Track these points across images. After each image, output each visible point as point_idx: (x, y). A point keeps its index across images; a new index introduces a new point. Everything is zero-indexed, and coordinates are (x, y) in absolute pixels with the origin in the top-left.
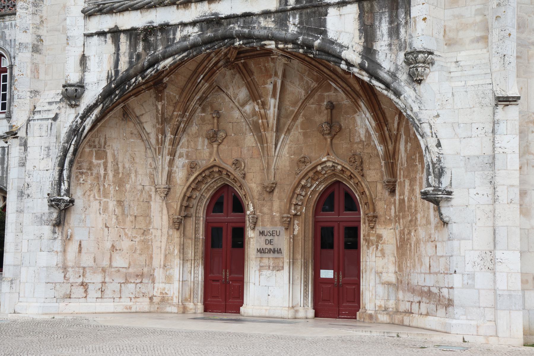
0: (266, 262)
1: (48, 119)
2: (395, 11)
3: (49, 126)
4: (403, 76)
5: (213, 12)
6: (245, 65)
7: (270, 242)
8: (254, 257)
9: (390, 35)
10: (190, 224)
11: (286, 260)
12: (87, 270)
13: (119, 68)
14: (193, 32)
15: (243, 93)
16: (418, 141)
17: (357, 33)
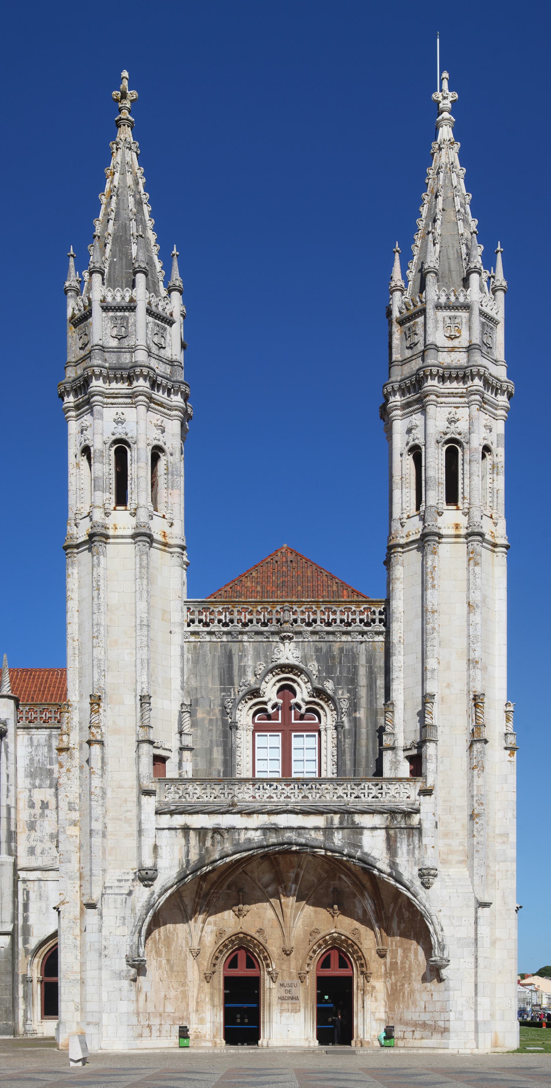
0: (285, 1006)
1: (122, 894)
2: (411, 840)
3: (124, 900)
4: (418, 882)
5: (273, 822)
7: (289, 991)
8: (276, 1003)
9: (408, 853)
12: (151, 1014)
13: (190, 858)
14: (256, 836)
16: (427, 927)
17: (385, 850)
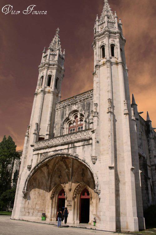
6: (65, 161)
10: (54, 199)
11: (73, 208)
14: (52, 153)
15: (65, 167)
